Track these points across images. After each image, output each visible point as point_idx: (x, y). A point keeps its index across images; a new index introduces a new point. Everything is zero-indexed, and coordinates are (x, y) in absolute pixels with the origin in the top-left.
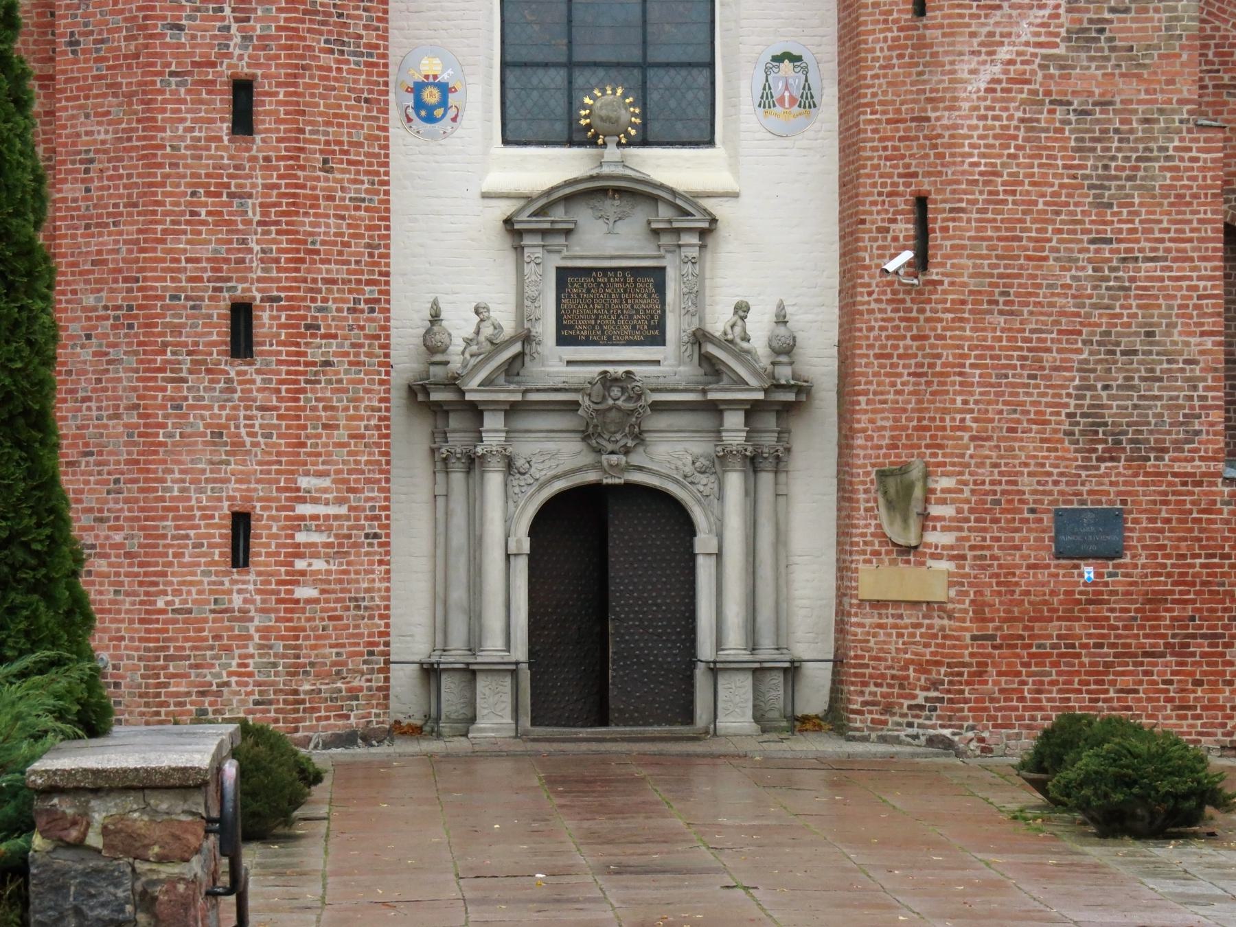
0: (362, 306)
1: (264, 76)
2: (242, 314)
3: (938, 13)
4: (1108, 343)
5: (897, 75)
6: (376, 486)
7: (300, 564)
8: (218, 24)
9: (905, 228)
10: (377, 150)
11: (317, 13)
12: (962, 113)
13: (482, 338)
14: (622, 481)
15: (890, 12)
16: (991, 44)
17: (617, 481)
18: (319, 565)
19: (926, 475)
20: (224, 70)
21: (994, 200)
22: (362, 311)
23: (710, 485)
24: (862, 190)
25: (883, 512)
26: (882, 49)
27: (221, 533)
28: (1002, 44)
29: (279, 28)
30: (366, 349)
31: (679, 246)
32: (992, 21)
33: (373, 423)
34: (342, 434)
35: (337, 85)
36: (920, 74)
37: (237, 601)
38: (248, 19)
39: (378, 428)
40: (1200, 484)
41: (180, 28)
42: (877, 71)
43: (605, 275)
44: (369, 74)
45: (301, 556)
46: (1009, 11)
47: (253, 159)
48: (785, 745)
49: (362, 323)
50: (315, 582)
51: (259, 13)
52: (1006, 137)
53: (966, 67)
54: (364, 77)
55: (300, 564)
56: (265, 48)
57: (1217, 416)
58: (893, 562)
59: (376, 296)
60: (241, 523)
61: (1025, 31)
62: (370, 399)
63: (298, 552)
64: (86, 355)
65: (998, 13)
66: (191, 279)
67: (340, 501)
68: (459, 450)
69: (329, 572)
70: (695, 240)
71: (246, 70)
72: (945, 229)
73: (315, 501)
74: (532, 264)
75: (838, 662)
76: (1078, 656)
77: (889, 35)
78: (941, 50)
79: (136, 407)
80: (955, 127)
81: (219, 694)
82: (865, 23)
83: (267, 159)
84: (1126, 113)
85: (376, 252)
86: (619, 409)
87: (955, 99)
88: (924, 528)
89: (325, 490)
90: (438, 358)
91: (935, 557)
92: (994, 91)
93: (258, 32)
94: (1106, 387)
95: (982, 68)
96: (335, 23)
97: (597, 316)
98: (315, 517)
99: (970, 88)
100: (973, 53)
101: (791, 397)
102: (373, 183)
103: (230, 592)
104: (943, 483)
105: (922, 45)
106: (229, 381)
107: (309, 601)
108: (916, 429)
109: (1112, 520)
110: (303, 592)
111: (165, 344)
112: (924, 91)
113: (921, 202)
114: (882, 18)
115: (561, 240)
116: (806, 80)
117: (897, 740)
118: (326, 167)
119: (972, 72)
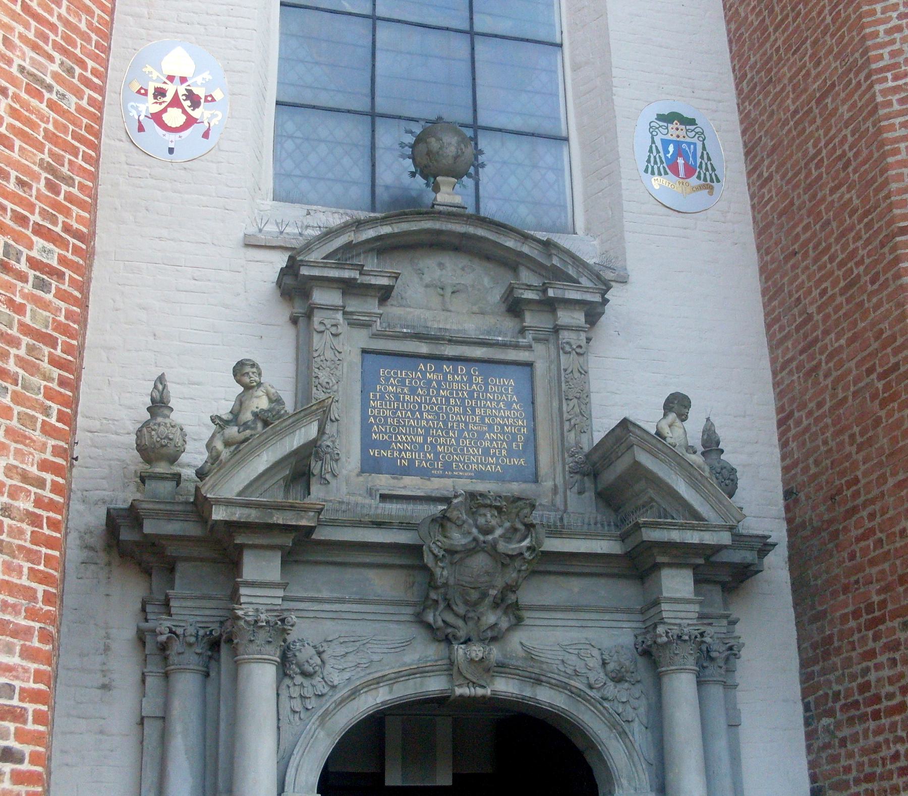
0: (23, 266)
6: (18, 643)
10: (83, 26)
13: (247, 416)
14: (488, 692)
17: (480, 692)
22: (23, 278)
23: (636, 703)
24: (894, 186)
30: (22, 352)
31: (556, 330)
33: (25, 504)
39: (35, 520)
42: (895, 22)
43: (439, 370)
49: (18, 299)
59: (54, 263)
62: (18, 453)
68: (191, 630)
70: (578, 318)
74: (327, 335)
85: (64, 188)
86: (492, 551)
90: (161, 468)
97: (427, 430)
101: (748, 556)
102: (70, 71)
115: (371, 306)
116: (704, 148)
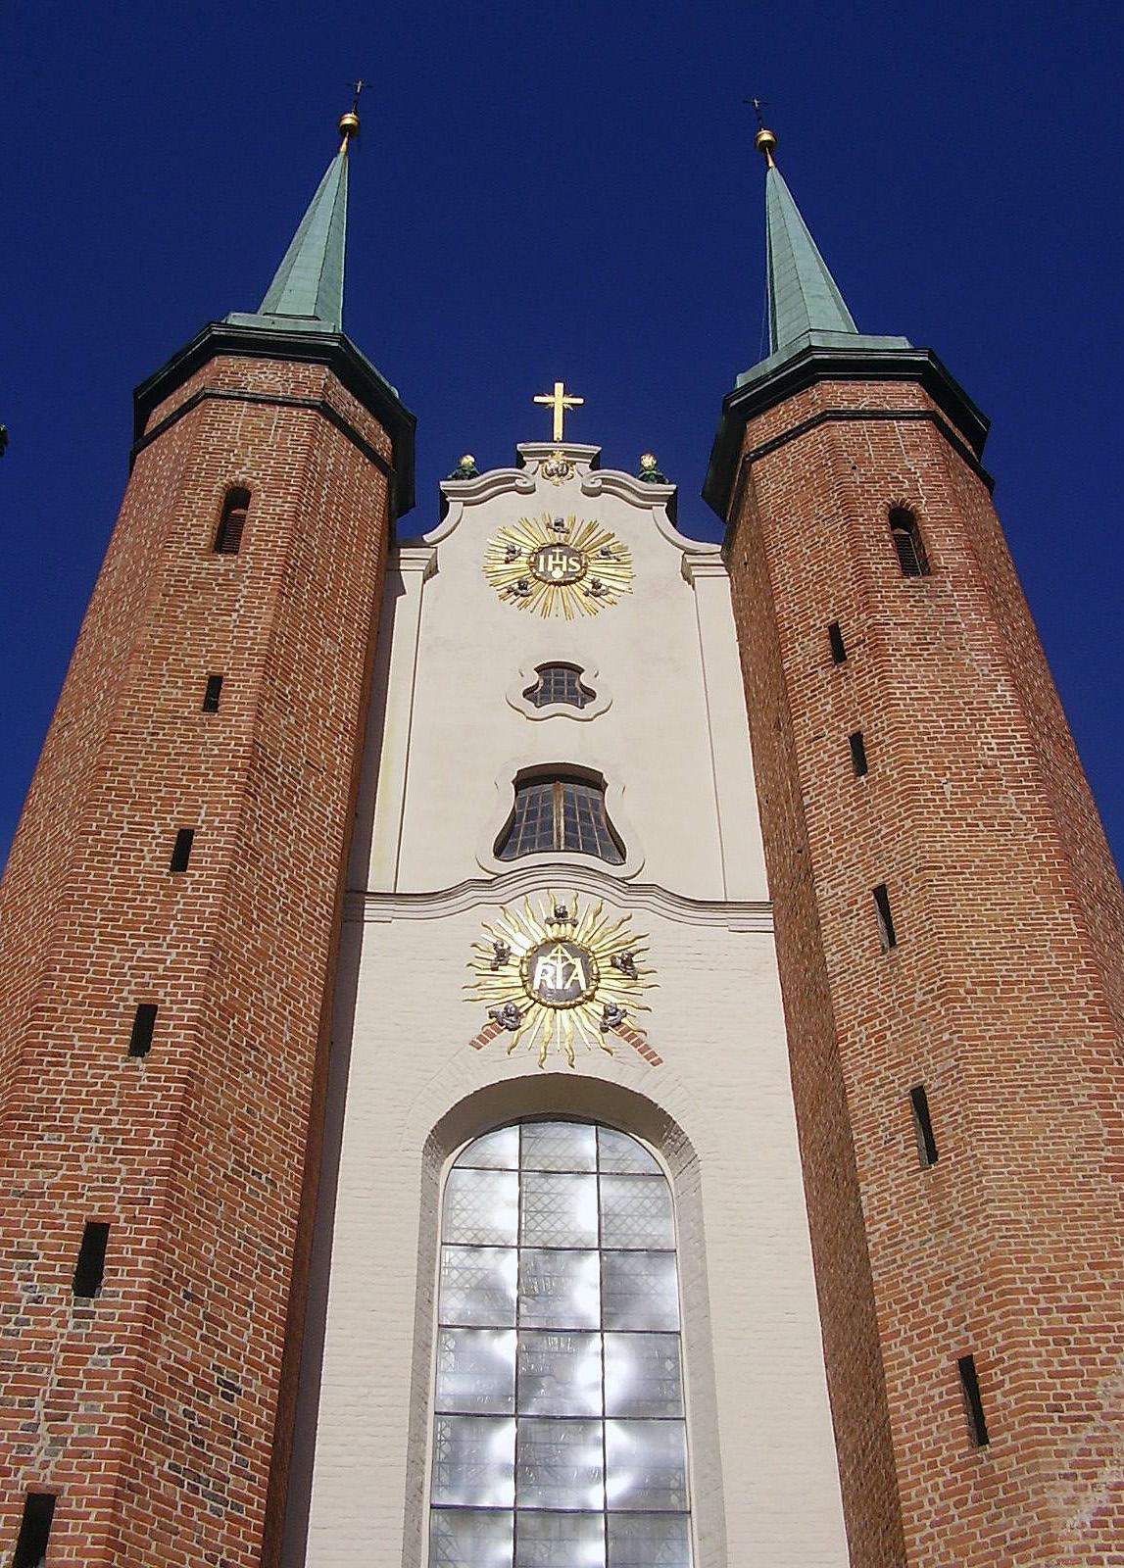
1: (72, 1491)
3: (1007, 1435)
5: (961, 1528)
8: (22, 1421)
11: (165, 1427)
12: (1065, 1556)
15: (938, 1452)
20: (21, 1481)
26: (932, 1502)
28: (1103, 1464)
29: (103, 1431)
32: (1082, 1435)
35: (181, 1528)
36: (997, 1516)
38: (64, 1418)
42: (929, 1530)
44: (233, 1531)
46: (1103, 1423)
51: (81, 1410)
53: (1061, 1496)
54: (225, 1532)
56: (80, 1455)
65: (1089, 1425)
71: (49, 1482)
77: (940, 1480)
78: (1018, 1479)
82: (904, 1474)
87: (1050, 1539)
92: (1105, 1524)
93: (75, 1434)
95: (1082, 1495)
96: (189, 1450)
99: (1069, 1522)
100: (1066, 1476)
105: (988, 1481)
112: (1003, 1540)
114: (925, 1462)
119: (1068, 1501)
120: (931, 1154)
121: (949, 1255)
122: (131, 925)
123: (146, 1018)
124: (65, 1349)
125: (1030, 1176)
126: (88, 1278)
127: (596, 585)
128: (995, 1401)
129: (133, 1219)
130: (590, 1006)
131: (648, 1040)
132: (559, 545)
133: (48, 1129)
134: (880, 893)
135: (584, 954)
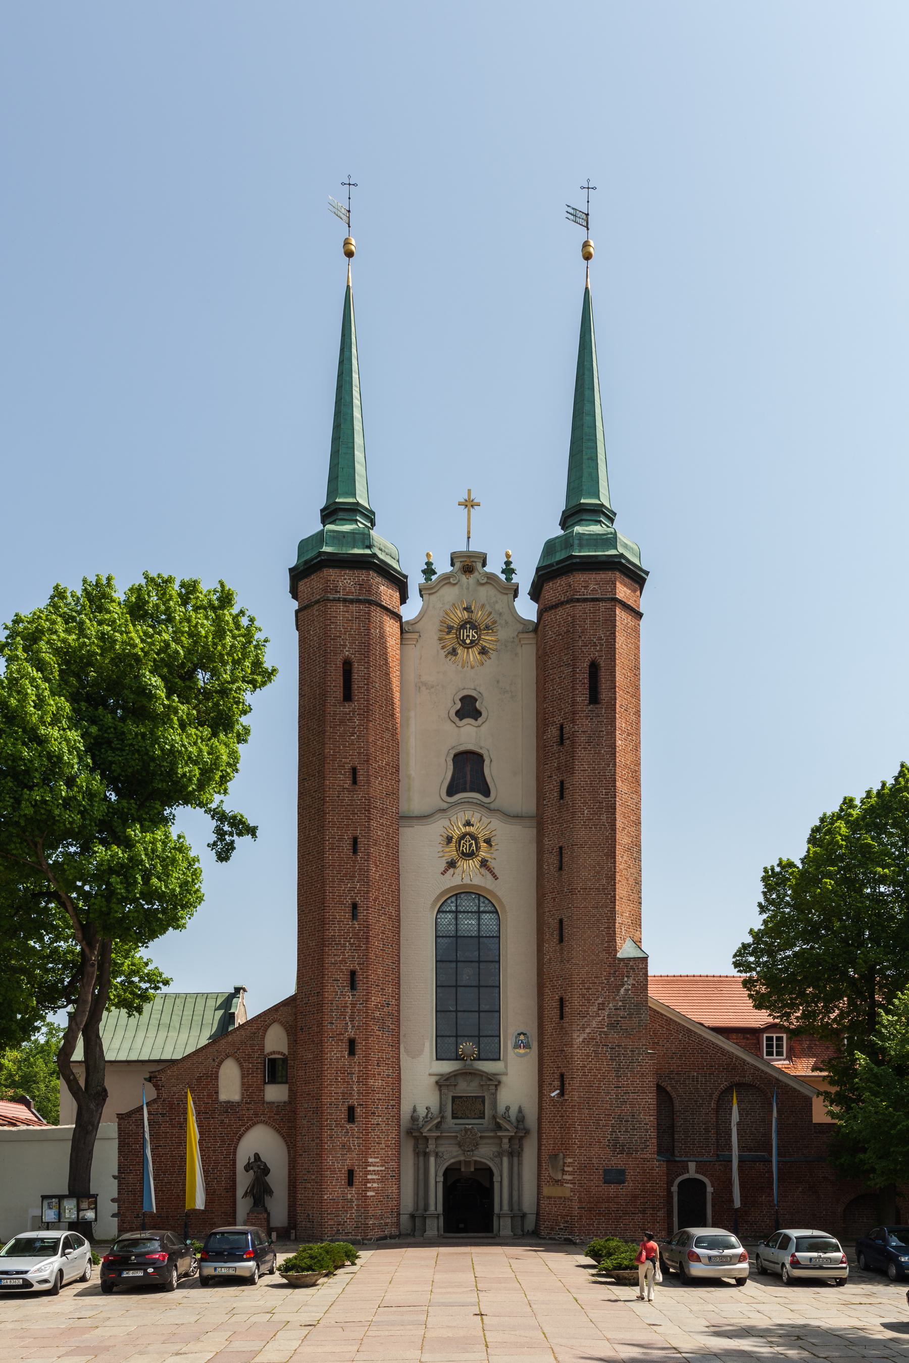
2: (351, 1110)
4: (620, 1118)
7: (369, 1185)
9: (557, 1083)
16: (583, 1028)
18: (375, 1185)
19: (564, 1158)
21: (584, 1075)
25: (550, 1169)
27: (344, 1176)
34: (383, 1146)
37: (349, 1196)
40: (649, 1161)
41: (333, 1023)
45: (370, 1183)
47: (355, 1062)
48: (519, 1241)
50: (374, 1191)
52: (588, 1056)
55: (369, 1185)
57: (654, 1141)
58: (554, 1185)
60: (351, 1173)
61: (594, 1024)
63: (368, 1181)
64: (305, 1122)
66: (335, 1099)
67: (382, 1166)
69: (378, 1187)
72: (569, 1084)
73: (374, 1166)
75: (538, 1214)
76: (611, 1214)
79: (319, 1138)
80: (572, 1052)
81: (344, 1225)
83: (359, 1063)
84: (625, 1048)
88: (563, 1174)
89: (377, 1163)
91: (566, 1183)
94: (619, 1132)
98: (374, 1171)
103: (347, 1194)
104: (570, 1160)
105: (562, 1028)
106: (347, 1129)
107: (372, 1196)
108: (561, 1144)
109: (622, 1172)
110: (370, 1194)
111: (328, 1119)
113: (562, 1076)
117: (554, 1239)
118: (378, 1065)
120: (561, 940)
121: (562, 970)
122: (345, 875)
123: (355, 906)
124: (351, 1004)
125: (584, 951)
126: (353, 987)
127: (483, 648)
128: (567, 1009)
129: (361, 969)
130: (478, 858)
131: (494, 871)
132: (469, 622)
133: (335, 944)
134: (561, 848)
135: (474, 837)
